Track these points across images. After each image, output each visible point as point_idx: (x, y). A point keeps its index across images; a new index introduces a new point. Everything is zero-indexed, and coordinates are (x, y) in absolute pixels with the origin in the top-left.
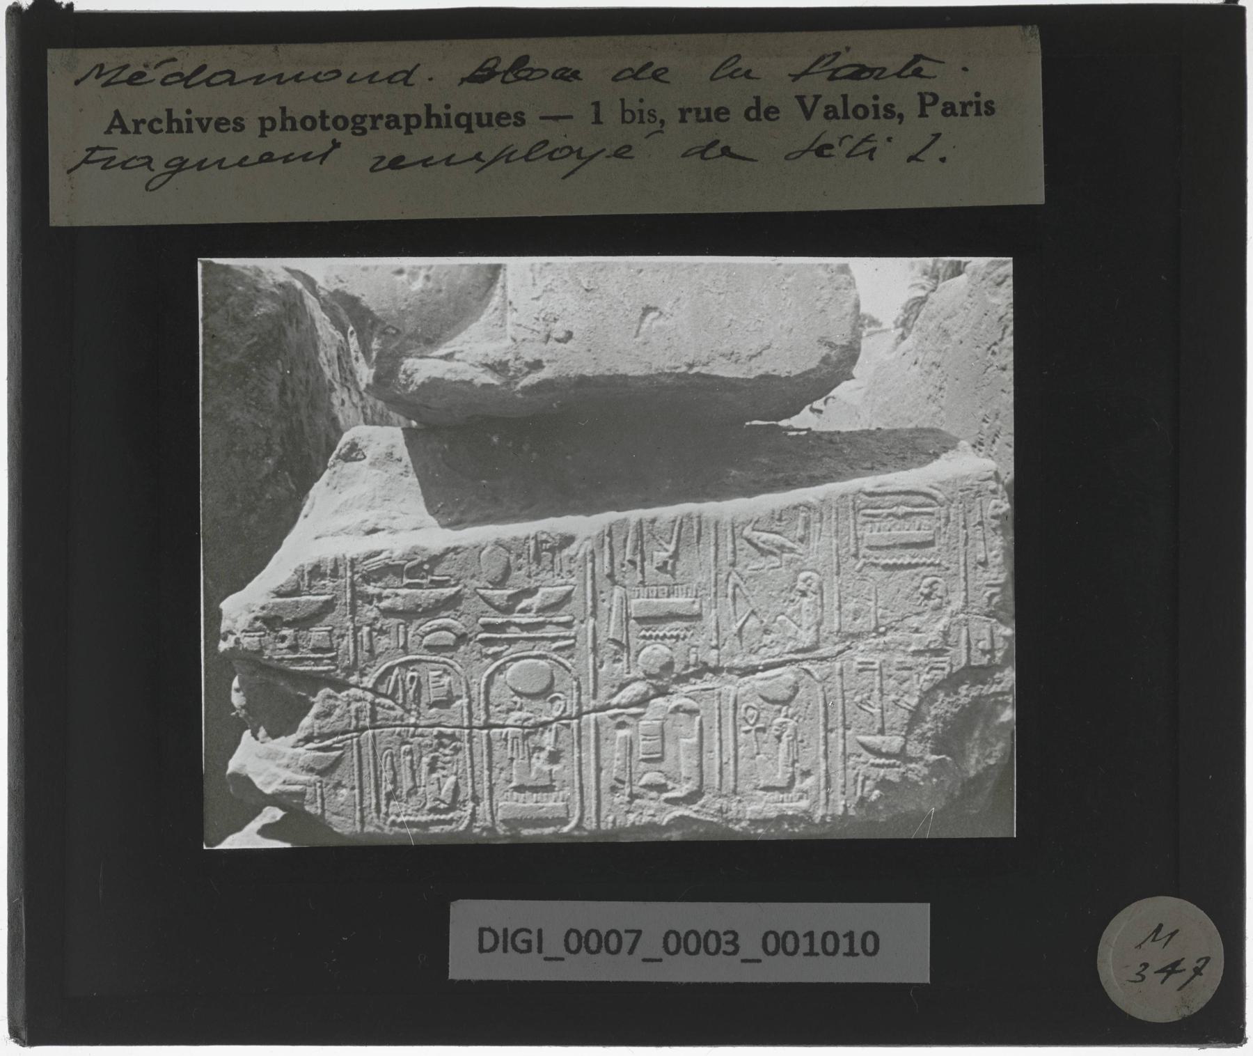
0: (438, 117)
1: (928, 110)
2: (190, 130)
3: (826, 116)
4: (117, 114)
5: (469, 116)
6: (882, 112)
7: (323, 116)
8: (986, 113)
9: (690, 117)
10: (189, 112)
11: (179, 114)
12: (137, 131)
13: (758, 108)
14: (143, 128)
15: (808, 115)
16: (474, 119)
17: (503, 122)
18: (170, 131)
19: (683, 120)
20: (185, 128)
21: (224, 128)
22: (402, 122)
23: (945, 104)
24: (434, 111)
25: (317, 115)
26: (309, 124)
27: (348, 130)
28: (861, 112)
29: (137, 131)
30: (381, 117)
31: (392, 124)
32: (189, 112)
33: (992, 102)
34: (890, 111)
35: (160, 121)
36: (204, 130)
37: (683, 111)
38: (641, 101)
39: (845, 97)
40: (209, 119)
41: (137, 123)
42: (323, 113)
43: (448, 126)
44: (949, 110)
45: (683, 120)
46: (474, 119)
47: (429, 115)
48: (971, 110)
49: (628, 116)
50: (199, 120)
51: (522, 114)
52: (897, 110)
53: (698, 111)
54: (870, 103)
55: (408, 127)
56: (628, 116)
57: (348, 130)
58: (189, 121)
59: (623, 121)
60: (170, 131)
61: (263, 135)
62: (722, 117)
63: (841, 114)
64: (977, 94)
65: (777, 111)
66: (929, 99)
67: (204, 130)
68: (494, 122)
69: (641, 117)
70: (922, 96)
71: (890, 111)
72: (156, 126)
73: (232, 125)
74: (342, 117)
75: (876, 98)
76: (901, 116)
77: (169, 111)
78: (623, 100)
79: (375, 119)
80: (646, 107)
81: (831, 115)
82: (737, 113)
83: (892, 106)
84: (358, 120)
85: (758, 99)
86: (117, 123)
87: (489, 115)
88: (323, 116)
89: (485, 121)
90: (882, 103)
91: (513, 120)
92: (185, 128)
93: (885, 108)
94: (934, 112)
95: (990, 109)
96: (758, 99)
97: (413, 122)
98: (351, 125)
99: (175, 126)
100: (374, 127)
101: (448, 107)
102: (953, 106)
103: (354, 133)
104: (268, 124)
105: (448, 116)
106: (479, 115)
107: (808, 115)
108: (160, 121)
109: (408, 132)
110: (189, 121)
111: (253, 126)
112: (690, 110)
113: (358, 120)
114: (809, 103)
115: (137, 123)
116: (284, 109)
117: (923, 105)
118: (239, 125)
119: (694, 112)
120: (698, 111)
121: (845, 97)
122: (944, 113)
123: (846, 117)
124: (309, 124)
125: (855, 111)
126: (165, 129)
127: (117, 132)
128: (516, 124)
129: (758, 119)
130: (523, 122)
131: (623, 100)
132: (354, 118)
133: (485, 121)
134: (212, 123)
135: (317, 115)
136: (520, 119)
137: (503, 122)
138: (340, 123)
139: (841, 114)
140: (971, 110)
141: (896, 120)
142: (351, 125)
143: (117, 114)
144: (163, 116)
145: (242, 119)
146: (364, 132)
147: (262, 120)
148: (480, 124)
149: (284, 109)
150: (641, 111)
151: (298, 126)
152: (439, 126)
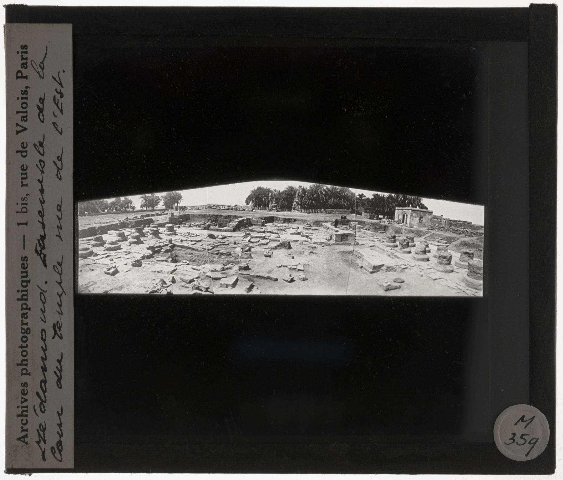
0: (22, 296)
1: (24, 75)
2: (27, 407)
3: (26, 121)
4: (19, 439)
5: (23, 281)
6: (25, 96)
7: (21, 347)
8: (26, 49)
9: (25, 182)
10: (18, 407)
11: (19, 411)
12: (27, 430)
13: (22, 152)
14: (25, 427)
15: (25, 129)
16: (24, 279)
17: (26, 266)
18: (27, 416)
19: (26, 185)
20: (25, 409)
21: (26, 392)
22: (25, 311)
23: (22, 67)
24: (21, 298)
25: (21, 350)
26: (24, 354)
27: (28, 336)
28: (24, 105)
29: (27, 430)
30: (22, 321)
31: (26, 316)
32: (18, 407)
33: (22, 46)
34: (25, 92)
35: (22, 420)
36: (26, 400)
37: (23, 185)
38: (17, 204)
39: (18, 112)
40: (22, 398)
41: (23, 430)
42: (20, 347)
43: (27, 291)
44: (24, 66)
45: (26, 185)
46: (24, 279)
47: (22, 299)
48: (25, 56)
49: (24, 210)
50: (22, 402)
51: (22, 258)
52: (24, 89)
53: (22, 178)
54: (21, 101)
55: (26, 309)
56: (24, 210)
57: (28, 336)
58: (22, 407)
59: (26, 212)
60: (27, 416)
61: (29, 374)
62: (25, 168)
63: (25, 114)
64: (18, 53)
65: (23, 143)
66: (19, 74)
67: (26, 400)
68: (26, 270)
69: (24, 204)
70: (18, 77)
71: (25, 92)
72: (24, 422)
73: (25, 388)
74: (22, 338)
75: (18, 98)
76: (27, 87)
77: (18, 416)
78: (17, 212)
79: (23, 324)
80: (20, 202)
81: (25, 119)
82: (25, 161)
83: (22, 91)
84: (23, 331)
85: (18, 152)
86: (23, 440)
87: (22, 272)
88: (21, 347)
89: (25, 274)
90: (21, 96)
91: (25, 262)
92: (25, 409)
93: (23, 94)
94: (25, 72)
95: (24, 47)
96: (18, 152)
97: (25, 306)
98: (25, 334)
99: (25, 413)
100: (27, 324)
101: (18, 291)
102: (23, 64)
103: (29, 333)
104: (24, 372)
105: (22, 291)
106: (23, 277)
107: (25, 129)
108: (22, 420)
109: (29, 309)
110: (22, 407)
111: (25, 379)
112: (22, 182)
113: (23, 331)
114: (19, 129)
115: (23, 430)
116: (18, 365)
117: (22, 77)
118: (25, 384)
119: (23, 180)
120: (22, 178)
121: (18, 112)
122: (26, 68)
123: (26, 112)
124: (24, 354)
125: (23, 108)
126: (26, 418)
127: (26, 440)
128: (27, 261)
129: (26, 152)
130: (26, 257)
131: (17, 212)
132: (23, 333)
133: (25, 274)
134: (24, 397)
135: (21, 350)
136: (25, 259)
137: (26, 266)
138: (25, 339)
139: (25, 114)
140: (25, 56)
141: (28, 89)
142: (25, 334)
143: (19, 439)
144: (21, 418)
145: (22, 383)
146: (28, 329)
147: (22, 374)
148: (26, 276)
149: (18, 365)
150: (22, 204)
151: (25, 358)
152: (26, 295)
